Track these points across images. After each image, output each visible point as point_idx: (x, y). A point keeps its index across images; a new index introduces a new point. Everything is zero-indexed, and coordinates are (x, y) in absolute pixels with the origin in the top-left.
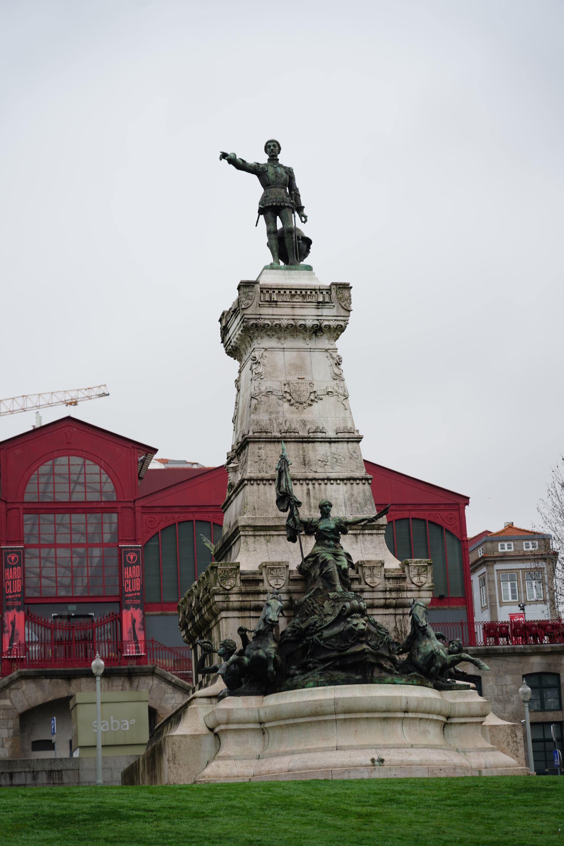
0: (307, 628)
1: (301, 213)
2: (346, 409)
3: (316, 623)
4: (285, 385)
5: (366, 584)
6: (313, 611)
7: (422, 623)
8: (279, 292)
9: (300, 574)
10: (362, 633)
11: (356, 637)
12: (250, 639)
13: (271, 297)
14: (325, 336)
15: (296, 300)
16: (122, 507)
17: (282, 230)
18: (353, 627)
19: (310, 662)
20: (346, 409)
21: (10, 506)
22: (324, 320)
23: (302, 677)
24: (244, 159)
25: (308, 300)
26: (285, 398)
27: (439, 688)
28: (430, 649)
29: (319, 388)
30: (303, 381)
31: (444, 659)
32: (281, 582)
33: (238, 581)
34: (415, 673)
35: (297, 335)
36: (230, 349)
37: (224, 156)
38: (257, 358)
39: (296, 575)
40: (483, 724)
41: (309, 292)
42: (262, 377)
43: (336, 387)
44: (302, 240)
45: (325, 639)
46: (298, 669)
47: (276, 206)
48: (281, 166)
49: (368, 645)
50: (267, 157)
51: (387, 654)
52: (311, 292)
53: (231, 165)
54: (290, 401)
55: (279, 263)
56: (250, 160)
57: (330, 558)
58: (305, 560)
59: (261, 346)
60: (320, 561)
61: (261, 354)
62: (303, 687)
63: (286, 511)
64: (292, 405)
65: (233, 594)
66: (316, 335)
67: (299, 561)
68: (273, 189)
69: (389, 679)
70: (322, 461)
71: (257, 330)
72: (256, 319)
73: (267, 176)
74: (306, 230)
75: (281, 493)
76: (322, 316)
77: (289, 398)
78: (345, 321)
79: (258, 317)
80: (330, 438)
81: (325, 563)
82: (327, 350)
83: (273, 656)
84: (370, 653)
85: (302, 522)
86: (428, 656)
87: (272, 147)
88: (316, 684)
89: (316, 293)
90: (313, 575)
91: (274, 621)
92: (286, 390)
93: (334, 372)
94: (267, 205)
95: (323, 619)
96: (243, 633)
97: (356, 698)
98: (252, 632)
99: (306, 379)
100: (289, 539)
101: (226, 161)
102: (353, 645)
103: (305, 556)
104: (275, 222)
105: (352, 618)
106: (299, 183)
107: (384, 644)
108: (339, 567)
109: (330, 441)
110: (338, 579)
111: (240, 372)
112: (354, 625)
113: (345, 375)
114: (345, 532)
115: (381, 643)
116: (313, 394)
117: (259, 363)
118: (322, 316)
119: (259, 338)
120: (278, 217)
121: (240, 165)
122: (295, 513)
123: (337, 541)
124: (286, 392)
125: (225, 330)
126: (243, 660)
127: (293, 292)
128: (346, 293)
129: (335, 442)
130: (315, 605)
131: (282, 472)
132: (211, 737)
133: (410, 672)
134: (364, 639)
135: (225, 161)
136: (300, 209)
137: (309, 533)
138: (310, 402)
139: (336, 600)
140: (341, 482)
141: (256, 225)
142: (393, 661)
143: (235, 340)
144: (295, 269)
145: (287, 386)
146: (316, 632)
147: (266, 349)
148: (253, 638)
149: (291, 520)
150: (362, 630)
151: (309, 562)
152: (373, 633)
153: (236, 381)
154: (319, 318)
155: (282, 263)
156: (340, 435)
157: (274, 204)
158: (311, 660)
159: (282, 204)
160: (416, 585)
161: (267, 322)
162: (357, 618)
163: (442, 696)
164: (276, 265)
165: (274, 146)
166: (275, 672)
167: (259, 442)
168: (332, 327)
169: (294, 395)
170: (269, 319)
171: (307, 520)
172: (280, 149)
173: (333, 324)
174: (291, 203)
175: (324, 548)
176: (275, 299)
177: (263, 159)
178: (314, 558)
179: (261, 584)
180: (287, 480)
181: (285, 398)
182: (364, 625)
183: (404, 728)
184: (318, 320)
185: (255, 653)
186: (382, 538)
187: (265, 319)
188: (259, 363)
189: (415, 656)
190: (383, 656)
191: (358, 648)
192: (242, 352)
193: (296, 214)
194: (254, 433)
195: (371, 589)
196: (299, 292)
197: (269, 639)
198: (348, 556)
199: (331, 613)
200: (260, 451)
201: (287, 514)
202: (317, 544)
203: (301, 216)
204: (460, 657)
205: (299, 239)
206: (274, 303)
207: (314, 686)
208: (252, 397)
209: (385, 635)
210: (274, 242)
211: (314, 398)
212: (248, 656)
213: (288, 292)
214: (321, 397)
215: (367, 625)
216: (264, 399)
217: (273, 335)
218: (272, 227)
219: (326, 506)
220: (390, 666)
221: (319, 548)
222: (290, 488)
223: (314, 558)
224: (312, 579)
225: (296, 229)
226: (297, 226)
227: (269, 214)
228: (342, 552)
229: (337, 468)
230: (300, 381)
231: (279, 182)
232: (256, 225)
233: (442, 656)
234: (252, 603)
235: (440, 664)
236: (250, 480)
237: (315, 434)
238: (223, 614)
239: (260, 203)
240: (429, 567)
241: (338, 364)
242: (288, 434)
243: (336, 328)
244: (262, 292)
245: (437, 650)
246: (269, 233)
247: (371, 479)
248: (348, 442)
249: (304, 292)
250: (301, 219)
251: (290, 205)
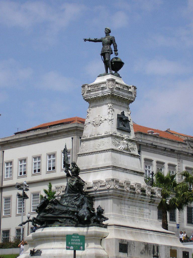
22: (104, 93)
29: (102, 119)
37: (85, 40)
56: (99, 38)
64: (95, 126)
74: (121, 57)
77: (94, 123)
109: (102, 137)
121: (96, 41)
124: (93, 122)
136: (116, 50)
161: (89, 98)
177: (104, 35)
187: (88, 97)
213: (93, 86)
229: (103, 147)
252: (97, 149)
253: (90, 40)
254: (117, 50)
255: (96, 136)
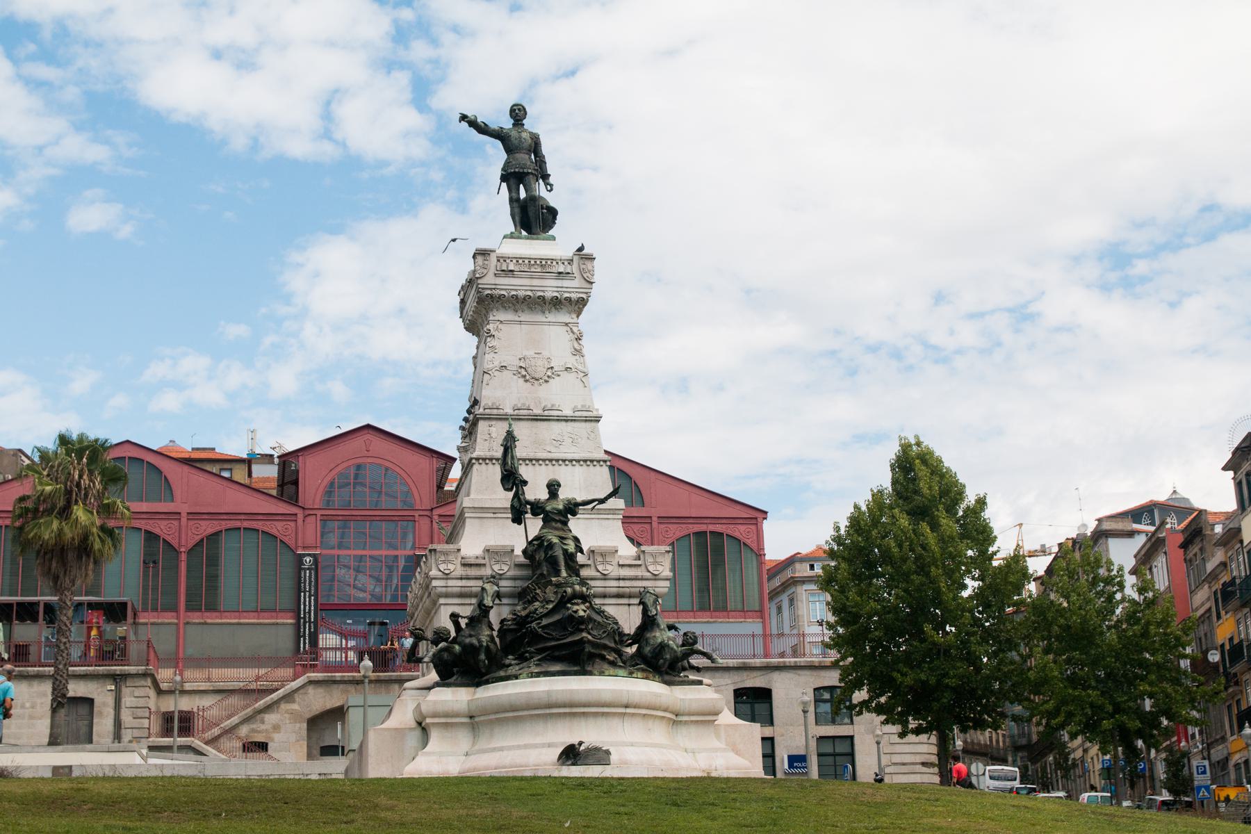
0: (527, 616)
1: (547, 181)
2: (586, 387)
3: (536, 609)
4: (520, 359)
5: (598, 571)
6: (534, 597)
7: (651, 612)
8: (517, 261)
9: (526, 558)
10: (582, 620)
11: (575, 625)
12: (463, 626)
13: (508, 267)
14: (565, 309)
15: (535, 270)
16: (419, 515)
17: (525, 199)
18: (573, 614)
19: (527, 652)
20: (586, 387)
21: (308, 512)
22: (564, 292)
23: (517, 668)
24: (487, 123)
25: (547, 271)
26: (519, 373)
27: (669, 683)
28: (659, 640)
30: (540, 356)
31: (675, 652)
32: (506, 568)
33: (459, 566)
34: (642, 666)
35: (535, 308)
36: (467, 324)
37: (464, 118)
38: (492, 330)
39: (522, 560)
40: (716, 723)
41: (549, 262)
42: (496, 351)
43: (575, 364)
44: (546, 209)
45: (544, 627)
46: (515, 660)
47: (519, 172)
48: (526, 131)
49: (589, 634)
50: (512, 121)
51: (613, 645)
52: (552, 263)
53: (472, 128)
54: (525, 376)
55: (521, 233)
56: (494, 126)
57: (555, 540)
58: (530, 543)
59: (496, 318)
60: (545, 544)
61: (495, 327)
62: (517, 678)
63: (511, 490)
64: (526, 381)
65: (453, 579)
66: (556, 309)
67: (524, 545)
68: (517, 154)
69: (612, 671)
70: (557, 441)
71: (492, 301)
72: (491, 289)
73: (510, 140)
74: (551, 199)
75: (506, 471)
76: (562, 287)
77: (524, 373)
78: (586, 293)
79: (493, 287)
80: (567, 417)
81: (551, 546)
82: (567, 324)
83: (485, 644)
84: (589, 641)
85: (528, 502)
86: (656, 648)
87: (517, 111)
88: (530, 675)
89: (557, 263)
90: (537, 559)
91: (488, 607)
92: (521, 365)
93: (573, 347)
94: (509, 171)
95: (544, 605)
96: (456, 619)
97: (572, 691)
98: (465, 618)
99: (543, 354)
100: (514, 521)
101: (466, 124)
102: (572, 634)
103: (530, 539)
104: (518, 189)
105: (573, 604)
106: (545, 149)
107: (608, 634)
108: (565, 551)
110: (563, 564)
111: (478, 348)
112: (573, 611)
113: (584, 351)
114: (574, 514)
115: (604, 632)
116: (550, 370)
117: (494, 336)
118: (562, 287)
119: (495, 310)
120: (521, 185)
121: (483, 129)
122: (520, 493)
123: (565, 523)
124: (521, 367)
125: (463, 302)
126: (454, 647)
127: (532, 262)
128: (588, 263)
129: (572, 420)
130: (538, 591)
131: (508, 448)
132: (418, 732)
133: (638, 664)
134: (583, 627)
135: (465, 124)
136: (545, 177)
137: (535, 514)
138: (547, 378)
139: (558, 585)
140: (577, 464)
141: (498, 193)
142: (620, 653)
143: (471, 313)
144: (537, 239)
145: (523, 360)
146: (536, 620)
147: (501, 322)
148: (466, 624)
149: (516, 500)
150: (582, 617)
151: (534, 545)
152: (595, 621)
153: (474, 357)
154: (559, 289)
155: (524, 233)
156: (577, 414)
157: (517, 170)
158: (529, 649)
159: (525, 171)
160: (653, 574)
162: (577, 604)
163: (672, 690)
164: (517, 234)
165: (519, 110)
166: (486, 662)
167: (489, 419)
168: (573, 299)
169: (529, 370)
170: (505, 289)
171: (533, 501)
172: (526, 114)
173: (574, 296)
174: (535, 170)
175: (551, 531)
176: (512, 269)
177: (507, 123)
178: (539, 541)
179: (483, 569)
180: (512, 458)
181: (519, 373)
182: (585, 611)
183: (625, 724)
184: (558, 292)
185: (468, 640)
186: (620, 523)
188: (494, 336)
189: (643, 648)
190: (605, 647)
191: (577, 638)
192: (480, 327)
193: (541, 181)
194: (485, 409)
195: (603, 577)
196: (538, 262)
197: (484, 627)
198: (576, 540)
199: (552, 599)
200: (490, 428)
201: (511, 494)
202: (542, 528)
203: (547, 184)
204: (692, 649)
205: (542, 208)
206: (511, 273)
207: (529, 677)
208: (484, 372)
209: (610, 624)
210: (517, 210)
211: (551, 373)
212: (459, 644)
214: (559, 373)
215: (588, 611)
216: (497, 373)
217: (509, 307)
218: (514, 195)
219: (554, 485)
220: (614, 657)
221: (545, 531)
222: (516, 465)
223: (539, 541)
224: (536, 564)
225: (540, 197)
226: (541, 195)
227: (512, 181)
228: (570, 535)
229: (573, 449)
230: (537, 356)
231: (523, 147)
232: (498, 193)
233: (672, 649)
234: (473, 588)
235: (668, 656)
236: (477, 459)
237: (550, 412)
238: (442, 601)
239: (502, 170)
240: (666, 554)
241: (578, 339)
242: (521, 411)
243: (578, 301)
244: (498, 261)
245: (666, 641)
246: (511, 200)
247: (610, 461)
248: (586, 421)
249: (544, 262)
250: (546, 188)
251: (533, 172)
252: (550, 452)
253: (473, 124)
254: (550, 175)
255: (537, 411)
